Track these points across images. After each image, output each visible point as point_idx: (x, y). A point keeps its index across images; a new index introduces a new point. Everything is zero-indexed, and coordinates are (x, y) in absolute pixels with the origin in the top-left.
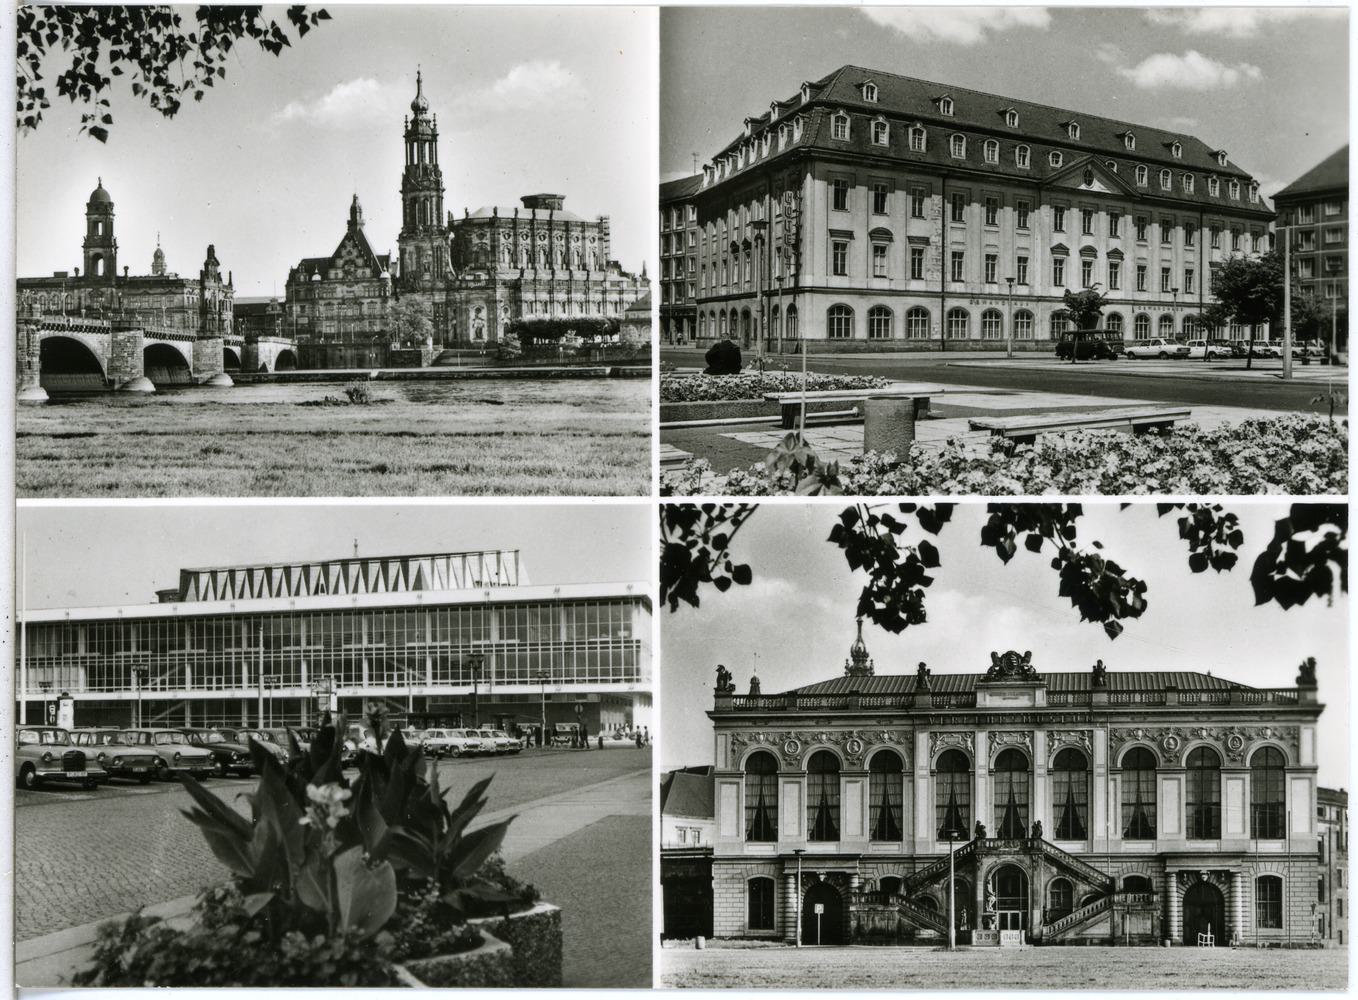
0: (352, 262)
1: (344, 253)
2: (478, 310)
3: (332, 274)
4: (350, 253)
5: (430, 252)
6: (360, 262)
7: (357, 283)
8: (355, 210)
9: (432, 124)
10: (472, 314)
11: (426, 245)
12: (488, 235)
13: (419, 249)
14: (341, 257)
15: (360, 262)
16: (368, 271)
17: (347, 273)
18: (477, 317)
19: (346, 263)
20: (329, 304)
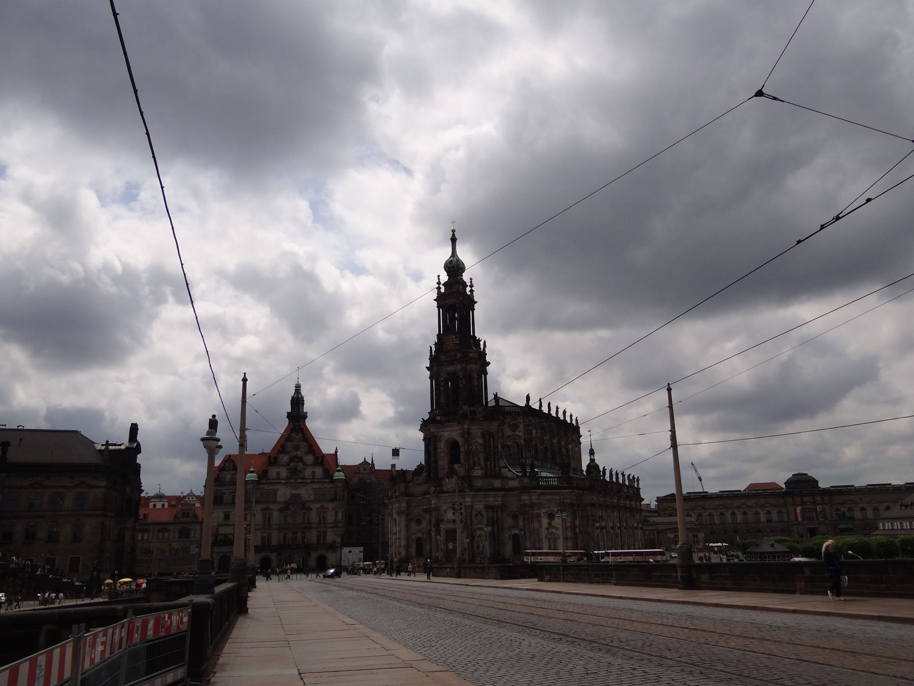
0: (301, 460)
1: (289, 445)
2: (551, 516)
3: (273, 472)
4: (297, 448)
5: (480, 441)
6: (309, 459)
7: (304, 484)
8: (297, 401)
9: (468, 289)
10: (545, 521)
11: (476, 431)
12: (521, 426)
13: (469, 433)
14: (286, 453)
15: (309, 459)
16: (319, 471)
17: (294, 472)
18: (550, 524)
19: (292, 460)
20: (268, 508)
